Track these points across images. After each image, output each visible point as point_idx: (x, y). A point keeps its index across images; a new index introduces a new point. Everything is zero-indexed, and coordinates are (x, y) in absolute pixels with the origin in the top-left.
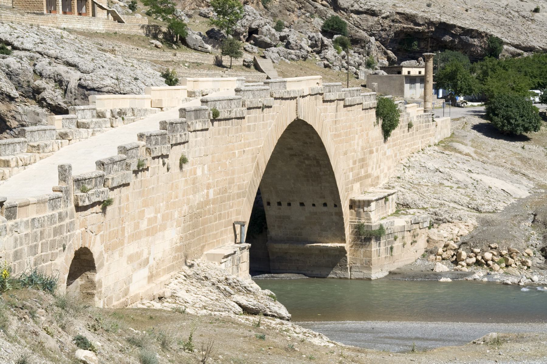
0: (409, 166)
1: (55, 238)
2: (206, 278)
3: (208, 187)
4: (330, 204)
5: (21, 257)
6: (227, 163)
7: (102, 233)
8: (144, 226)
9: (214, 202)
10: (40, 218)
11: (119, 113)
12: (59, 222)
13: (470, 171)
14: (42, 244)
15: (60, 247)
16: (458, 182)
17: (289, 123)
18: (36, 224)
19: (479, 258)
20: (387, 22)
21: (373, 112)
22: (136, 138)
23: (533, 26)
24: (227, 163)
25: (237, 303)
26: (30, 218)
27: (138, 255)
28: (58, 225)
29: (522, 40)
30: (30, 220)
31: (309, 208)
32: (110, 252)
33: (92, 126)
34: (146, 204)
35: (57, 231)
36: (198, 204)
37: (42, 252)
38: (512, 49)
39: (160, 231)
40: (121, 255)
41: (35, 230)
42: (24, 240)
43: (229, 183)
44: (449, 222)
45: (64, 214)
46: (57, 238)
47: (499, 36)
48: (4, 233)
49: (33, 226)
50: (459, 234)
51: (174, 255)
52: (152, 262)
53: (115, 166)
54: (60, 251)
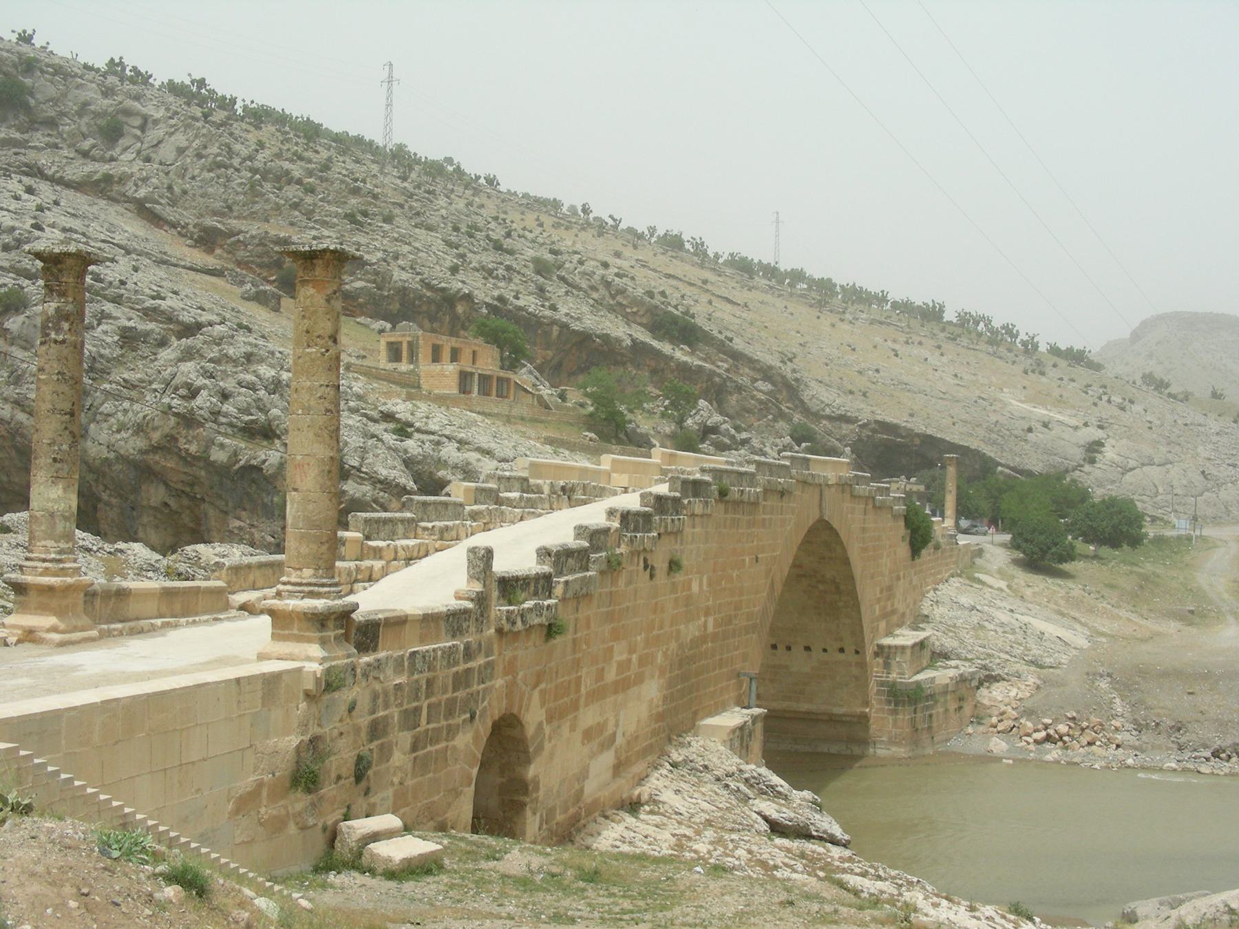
0: (937, 602)
1: (455, 695)
2: (706, 767)
3: (707, 614)
4: (850, 649)
5: (385, 733)
6: (735, 575)
7: (543, 686)
8: (611, 675)
9: (715, 637)
10: (427, 651)
12: (465, 662)
13: (1012, 611)
14: (429, 706)
15: (465, 712)
16: (1002, 625)
19: (1051, 732)
21: (902, 523)
22: (604, 516)
23: (1027, 447)
24: (735, 575)
25: (759, 813)
27: (601, 727)
28: (461, 667)
29: (1016, 461)
31: (817, 654)
32: (555, 723)
34: (616, 635)
35: (461, 680)
36: (691, 640)
37: (428, 723)
39: (635, 684)
40: (573, 729)
41: (416, 676)
42: (392, 698)
43: (737, 609)
44: (1004, 679)
46: (461, 694)
47: (992, 455)
48: (350, 680)
50: (1018, 697)
51: (653, 726)
52: (620, 740)
53: (570, 560)
54: (464, 721)
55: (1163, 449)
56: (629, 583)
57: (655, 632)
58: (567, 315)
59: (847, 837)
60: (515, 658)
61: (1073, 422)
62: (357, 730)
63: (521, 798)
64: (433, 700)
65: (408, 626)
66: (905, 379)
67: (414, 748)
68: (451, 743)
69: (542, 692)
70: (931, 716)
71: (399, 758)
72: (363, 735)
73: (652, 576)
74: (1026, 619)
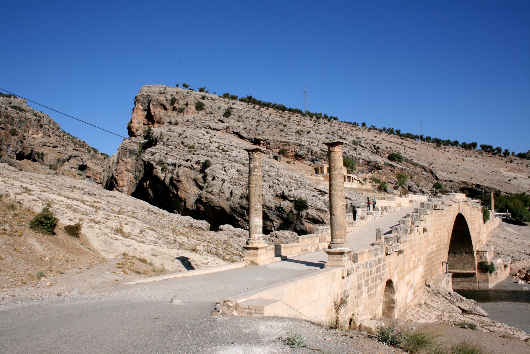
3: (433, 244)
5: (361, 288)
7: (397, 270)
8: (412, 265)
9: (435, 251)
11: (385, 209)
14: (371, 278)
17: (457, 214)
18: (368, 266)
20: (457, 185)
23: (510, 186)
26: (364, 262)
27: (410, 281)
28: (378, 266)
29: (507, 191)
30: (365, 263)
32: (400, 281)
33: (374, 214)
34: (412, 254)
35: (378, 270)
38: (504, 194)
45: (381, 259)
46: (378, 274)
49: (367, 267)
52: (414, 286)
54: (380, 282)
56: (414, 236)
57: (421, 251)
59: (488, 314)
60: (390, 262)
62: (355, 287)
63: (393, 305)
64: (372, 276)
65: (365, 254)
67: (368, 292)
68: (376, 289)
69: (397, 272)
70: (496, 273)
71: (365, 295)
72: (356, 289)
73: (419, 234)
74: (523, 241)
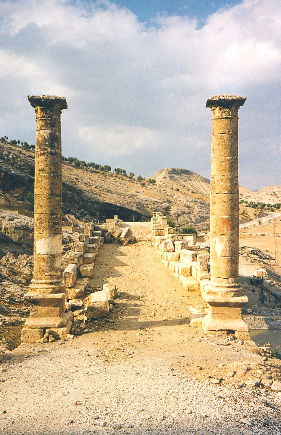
55: (188, 209)
58: (5, 169)
61: (161, 202)
66: (110, 189)
